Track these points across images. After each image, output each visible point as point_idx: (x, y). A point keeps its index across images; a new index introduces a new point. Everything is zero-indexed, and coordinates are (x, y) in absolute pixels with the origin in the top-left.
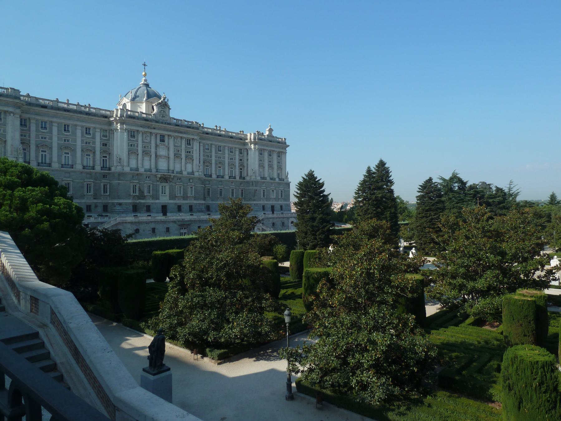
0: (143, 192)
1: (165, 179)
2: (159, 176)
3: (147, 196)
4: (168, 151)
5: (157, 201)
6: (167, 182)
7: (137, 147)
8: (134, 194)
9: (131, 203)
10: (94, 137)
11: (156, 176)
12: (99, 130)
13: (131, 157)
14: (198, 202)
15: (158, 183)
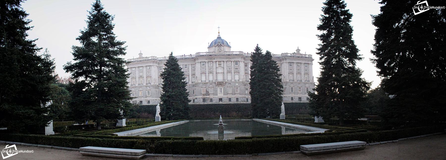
0: (208, 92)
1: (220, 84)
2: (216, 83)
3: (210, 94)
4: (224, 69)
5: (216, 96)
6: (222, 86)
7: (206, 70)
8: (204, 93)
9: (202, 98)
10: (188, 69)
11: (215, 83)
12: (191, 65)
13: (202, 75)
14: (242, 96)
15: (217, 87)
